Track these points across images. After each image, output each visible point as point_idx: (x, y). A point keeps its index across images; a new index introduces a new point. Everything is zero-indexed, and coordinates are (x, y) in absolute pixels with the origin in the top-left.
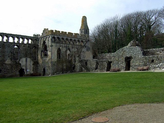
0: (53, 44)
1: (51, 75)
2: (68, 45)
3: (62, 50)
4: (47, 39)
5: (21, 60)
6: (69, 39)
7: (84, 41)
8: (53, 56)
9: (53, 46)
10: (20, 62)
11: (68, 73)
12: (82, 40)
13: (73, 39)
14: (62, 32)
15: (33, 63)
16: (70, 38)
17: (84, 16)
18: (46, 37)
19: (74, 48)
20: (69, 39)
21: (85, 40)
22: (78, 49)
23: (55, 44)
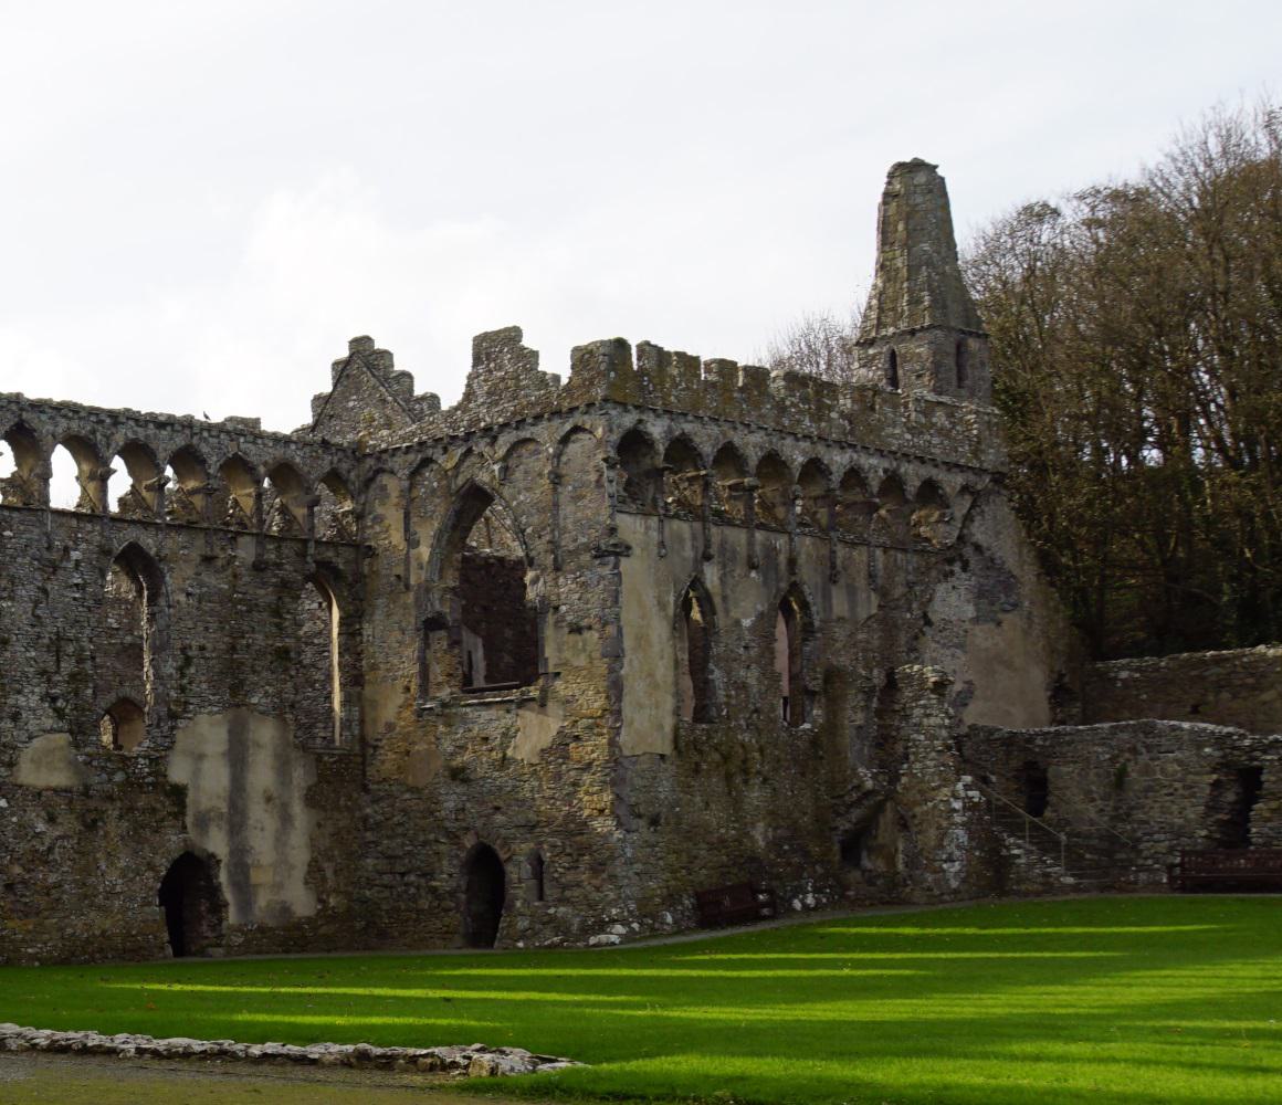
0: (632, 527)
1: (619, 928)
2: (781, 542)
3: (725, 598)
4: (536, 463)
5: (179, 735)
6: (797, 455)
7: (952, 482)
8: (635, 689)
9: (622, 550)
10: (178, 772)
11: (805, 906)
12: (927, 471)
13: (838, 460)
14: (726, 368)
15: (313, 780)
16: (805, 445)
17: (917, 166)
18: (505, 441)
19: (842, 581)
20: (797, 455)
21: (959, 480)
22: (884, 593)
23: (653, 522)
